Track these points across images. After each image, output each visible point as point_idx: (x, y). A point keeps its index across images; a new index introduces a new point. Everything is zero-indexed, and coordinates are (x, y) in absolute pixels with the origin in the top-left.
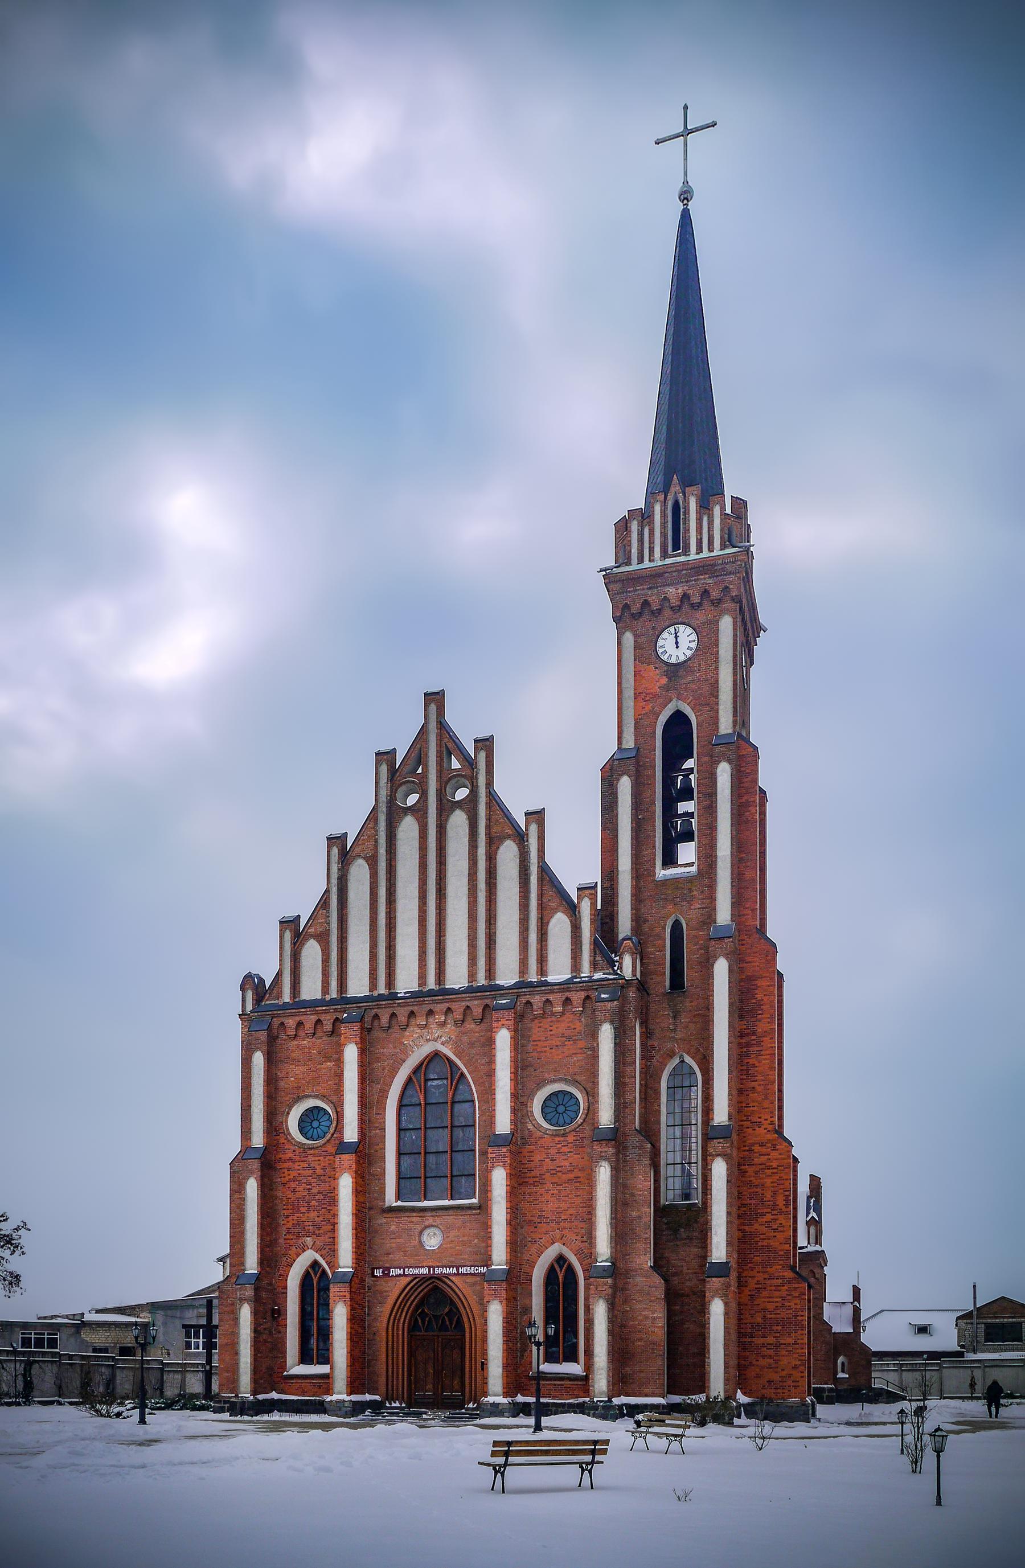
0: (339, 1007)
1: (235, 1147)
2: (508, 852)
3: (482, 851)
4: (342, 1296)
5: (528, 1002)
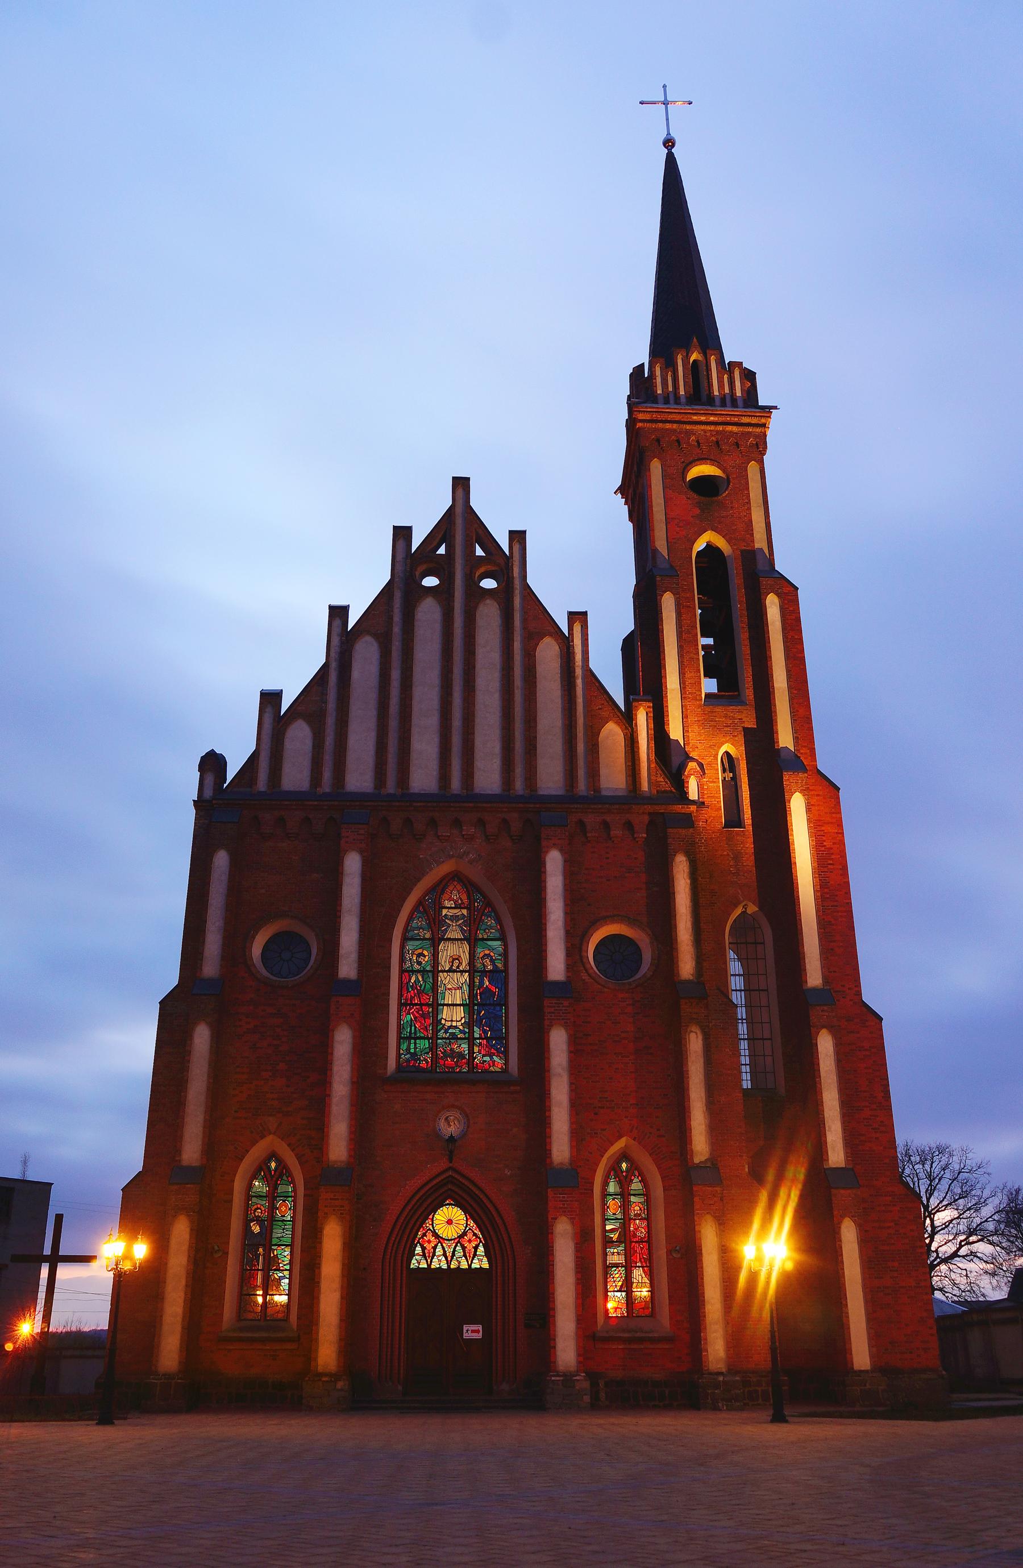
0: (336, 803)
1: (170, 978)
2: (548, 651)
3: (517, 645)
4: (336, 1206)
5: (581, 823)
